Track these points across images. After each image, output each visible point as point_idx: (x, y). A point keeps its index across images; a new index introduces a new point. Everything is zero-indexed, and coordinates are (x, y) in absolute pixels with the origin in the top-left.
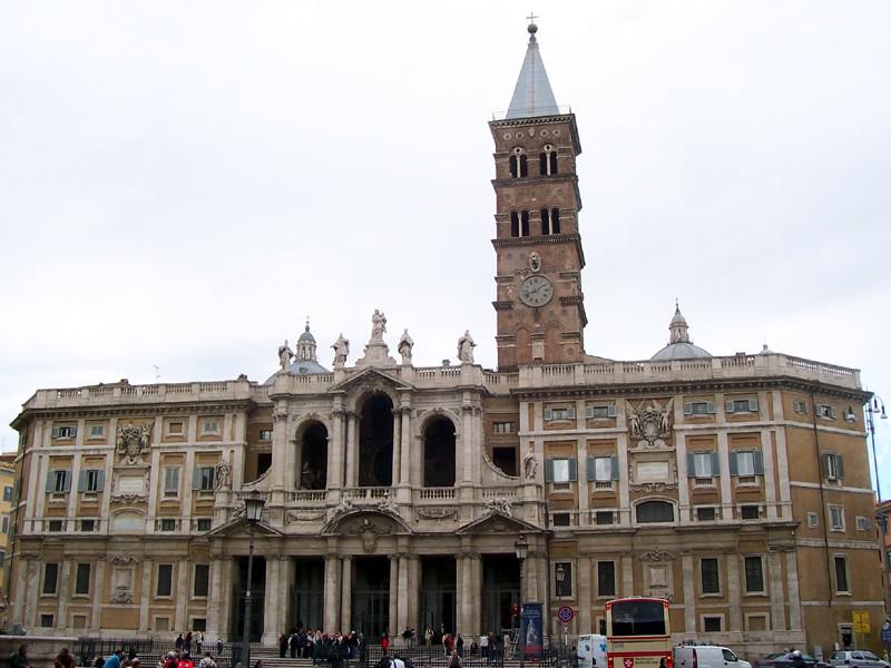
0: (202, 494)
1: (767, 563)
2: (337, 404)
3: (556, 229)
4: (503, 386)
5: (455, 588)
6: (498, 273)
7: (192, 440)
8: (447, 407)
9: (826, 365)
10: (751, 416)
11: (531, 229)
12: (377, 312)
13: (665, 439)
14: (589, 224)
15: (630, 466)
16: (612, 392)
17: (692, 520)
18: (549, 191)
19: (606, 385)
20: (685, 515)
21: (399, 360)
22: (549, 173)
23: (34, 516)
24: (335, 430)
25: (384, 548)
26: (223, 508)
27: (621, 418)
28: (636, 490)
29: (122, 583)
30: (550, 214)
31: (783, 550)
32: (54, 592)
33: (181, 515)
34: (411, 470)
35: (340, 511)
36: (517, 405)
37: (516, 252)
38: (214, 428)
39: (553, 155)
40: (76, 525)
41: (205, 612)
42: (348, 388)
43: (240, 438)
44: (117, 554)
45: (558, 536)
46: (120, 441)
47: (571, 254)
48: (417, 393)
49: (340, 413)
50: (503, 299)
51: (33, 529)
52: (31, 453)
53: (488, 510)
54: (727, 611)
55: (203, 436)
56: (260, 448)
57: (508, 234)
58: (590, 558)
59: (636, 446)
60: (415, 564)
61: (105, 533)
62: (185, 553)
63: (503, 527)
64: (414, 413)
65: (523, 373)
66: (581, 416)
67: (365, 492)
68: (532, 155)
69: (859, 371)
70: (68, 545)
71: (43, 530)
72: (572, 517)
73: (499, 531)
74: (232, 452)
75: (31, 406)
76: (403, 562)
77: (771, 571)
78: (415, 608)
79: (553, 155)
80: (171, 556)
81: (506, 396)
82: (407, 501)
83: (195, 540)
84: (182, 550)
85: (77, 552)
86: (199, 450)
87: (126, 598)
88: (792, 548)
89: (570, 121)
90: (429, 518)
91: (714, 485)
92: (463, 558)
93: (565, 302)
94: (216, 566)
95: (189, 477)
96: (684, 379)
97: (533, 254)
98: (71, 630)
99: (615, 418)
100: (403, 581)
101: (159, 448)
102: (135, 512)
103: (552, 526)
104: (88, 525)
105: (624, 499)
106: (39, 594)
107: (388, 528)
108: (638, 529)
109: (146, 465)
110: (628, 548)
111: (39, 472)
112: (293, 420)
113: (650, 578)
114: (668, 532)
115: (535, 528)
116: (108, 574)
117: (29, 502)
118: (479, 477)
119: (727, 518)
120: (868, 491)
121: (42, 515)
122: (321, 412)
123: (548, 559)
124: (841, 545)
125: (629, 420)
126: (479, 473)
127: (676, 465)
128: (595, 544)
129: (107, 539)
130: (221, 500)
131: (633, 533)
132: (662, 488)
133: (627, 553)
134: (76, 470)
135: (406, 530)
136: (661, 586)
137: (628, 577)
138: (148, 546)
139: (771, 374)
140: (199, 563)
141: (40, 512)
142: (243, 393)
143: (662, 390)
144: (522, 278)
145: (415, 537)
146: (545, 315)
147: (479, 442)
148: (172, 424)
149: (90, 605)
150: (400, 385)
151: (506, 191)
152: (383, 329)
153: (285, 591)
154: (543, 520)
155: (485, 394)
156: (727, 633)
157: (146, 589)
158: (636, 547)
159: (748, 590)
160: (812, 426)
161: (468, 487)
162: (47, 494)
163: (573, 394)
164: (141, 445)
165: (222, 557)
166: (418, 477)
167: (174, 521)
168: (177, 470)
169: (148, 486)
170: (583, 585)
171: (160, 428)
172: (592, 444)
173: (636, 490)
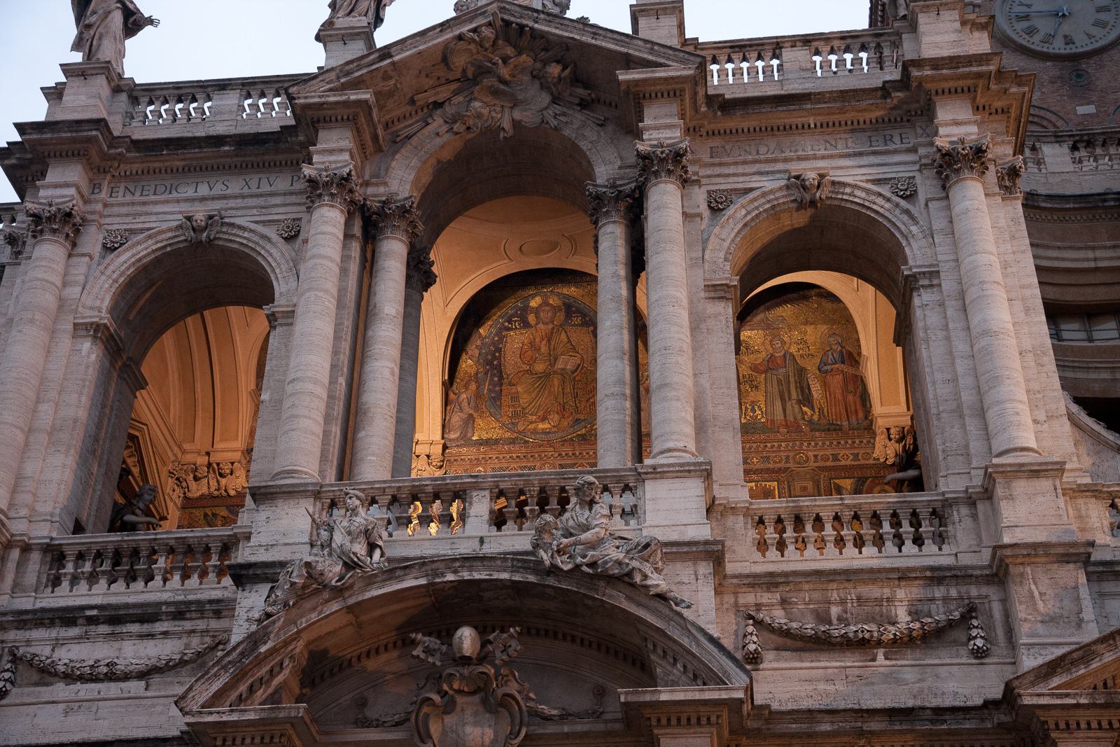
35: (314, 584)
107: (581, 701)
112: (109, 249)
135: (701, 675)
161: (1035, 473)
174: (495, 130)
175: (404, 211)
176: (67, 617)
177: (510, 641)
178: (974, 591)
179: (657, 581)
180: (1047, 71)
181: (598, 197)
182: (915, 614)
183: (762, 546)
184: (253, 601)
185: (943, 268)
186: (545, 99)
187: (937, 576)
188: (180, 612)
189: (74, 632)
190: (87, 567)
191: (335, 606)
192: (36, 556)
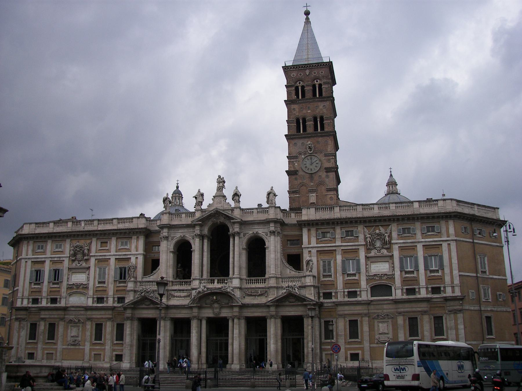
0: (120, 282)
1: (446, 319)
2: (197, 230)
3: (322, 128)
4: (293, 219)
5: (266, 336)
6: (289, 154)
7: (113, 252)
8: (261, 231)
9: (479, 205)
10: (436, 235)
11: (308, 128)
12: (219, 177)
14: (340, 124)
15: (366, 265)
16: (356, 222)
17: (403, 295)
18: (317, 107)
19: (353, 218)
20: (399, 292)
21: (233, 204)
22: (318, 96)
23: (23, 296)
24: (196, 245)
25: (225, 313)
26: (132, 290)
27: (361, 237)
28: (370, 278)
29: (74, 333)
30: (318, 120)
31: (456, 312)
32: (35, 339)
33: (108, 294)
34: (240, 268)
35: (199, 292)
36: (301, 230)
37: (299, 142)
38: (126, 244)
39: (320, 85)
40: (47, 301)
41: (122, 350)
42: (203, 221)
43: (141, 250)
44: (71, 317)
45: (325, 305)
46: (72, 252)
47: (331, 143)
48: (243, 224)
49: (199, 235)
50: (292, 169)
51: (22, 303)
52: (21, 259)
53: (285, 291)
55: (120, 249)
56: (154, 256)
57: (294, 131)
58: (344, 318)
60: (243, 322)
61: (64, 306)
62: (111, 316)
63: (293, 300)
64: (242, 235)
65: (304, 211)
66: (338, 236)
67: (214, 280)
68: (308, 86)
69: (498, 208)
70: (43, 313)
71: (28, 303)
72: (333, 294)
73: (291, 302)
74: (137, 258)
75: (20, 232)
76: (236, 321)
77: (448, 324)
78: (243, 347)
79: (320, 85)
80: (102, 318)
81: (294, 225)
82: (238, 286)
83: (116, 309)
84: (108, 314)
85: (48, 316)
86: (117, 257)
87: (77, 342)
88: (460, 311)
89: (329, 65)
90: (251, 295)
91: (415, 275)
92: (271, 318)
93: (328, 170)
94: (128, 324)
95: (112, 273)
96: (397, 214)
97: (309, 142)
98: (45, 361)
99: (358, 236)
100: (236, 332)
101: (94, 256)
102: (81, 293)
103: (322, 300)
104: (54, 301)
105: (363, 284)
106: (26, 340)
108: (372, 301)
109: (87, 266)
110: (366, 312)
111: (25, 270)
113: (379, 329)
114: (389, 302)
115: (312, 300)
116: (66, 329)
117: (20, 288)
118: (279, 271)
119: (423, 294)
120: (504, 278)
121: (27, 295)
122: (188, 234)
123: (320, 318)
124: (489, 309)
125: (366, 238)
126: (279, 269)
127: (393, 263)
128: (347, 310)
129: (65, 309)
130: (130, 286)
131: (368, 303)
132: (385, 278)
133: (366, 315)
134: (47, 268)
135: (238, 303)
136: (385, 333)
137: (366, 328)
138: (89, 313)
139: (448, 211)
140: (119, 322)
141: (26, 294)
142: (142, 224)
143: (385, 220)
144: (303, 157)
145: (243, 306)
146: (316, 178)
147: (279, 251)
148: (101, 242)
149: (56, 347)
150: (233, 219)
151: (293, 106)
152: (223, 187)
153: (168, 338)
154: (316, 296)
155: (282, 224)
157: (88, 338)
158: (370, 311)
159: (435, 335)
160: (471, 240)
162: (30, 283)
163: (333, 223)
164: (84, 255)
165: (132, 319)
166: (244, 272)
167: (103, 298)
168: (105, 269)
169: (88, 278)
170: (341, 333)
171: (95, 245)
172: (345, 252)
173: (370, 278)
174: (217, 223)
175: (206, 236)
176: (175, 290)
177: (219, 298)
178: (267, 290)
179: (233, 293)
180: (308, 176)
181: (230, 234)
182: (261, 292)
183: (246, 283)
184: (194, 292)
185: (269, 247)
186: (223, 218)
187: (263, 288)
188: (186, 290)
189: (176, 292)
191: (202, 294)
192: (170, 282)
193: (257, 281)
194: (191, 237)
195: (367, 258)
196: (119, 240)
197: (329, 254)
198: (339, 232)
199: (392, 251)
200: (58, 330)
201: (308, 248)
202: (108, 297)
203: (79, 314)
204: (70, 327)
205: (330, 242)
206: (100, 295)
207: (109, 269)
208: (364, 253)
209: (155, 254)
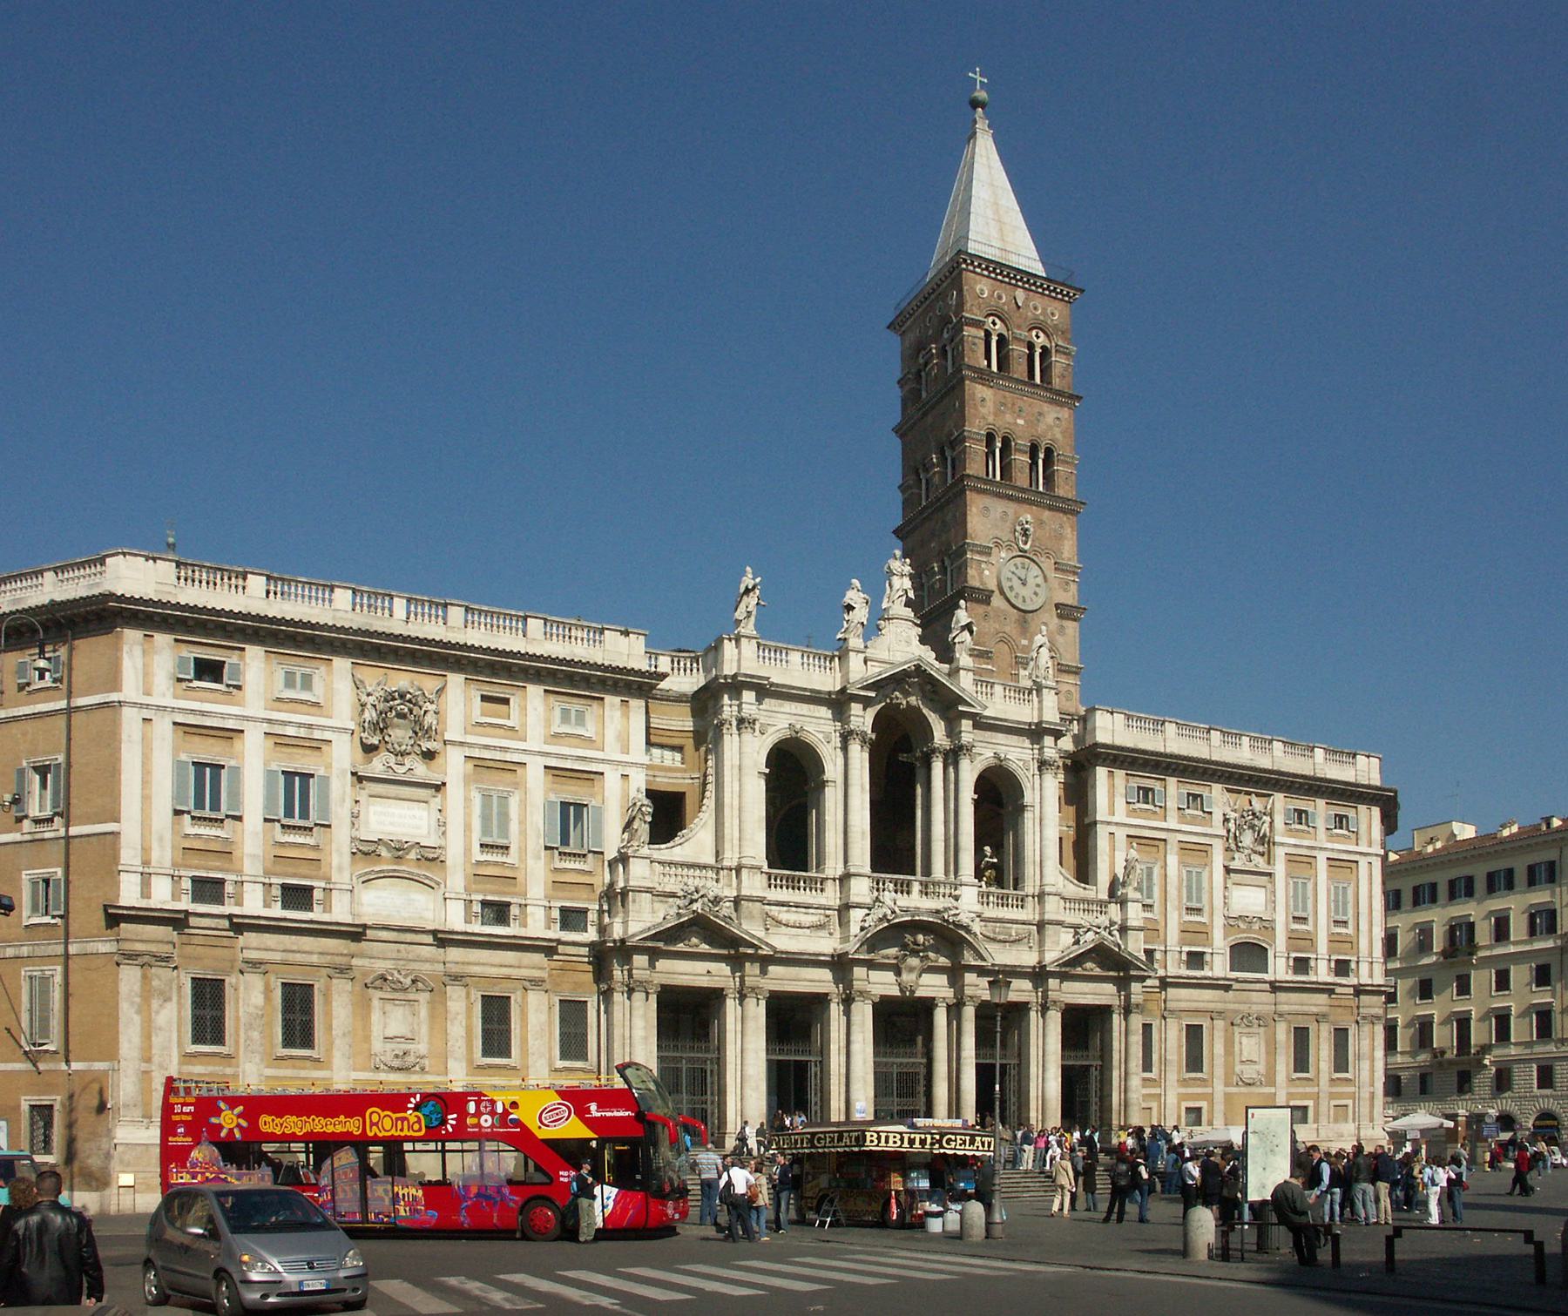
7: (535, 741)
8: (1018, 754)
13: (1262, 854)
17: (1287, 973)
20: (1281, 963)
26: (649, 890)
28: (1232, 923)
33: (525, 895)
44: (381, 966)
54: (1317, 1098)
55: (557, 735)
59: (1234, 859)
66: (1172, 804)
67: (908, 886)
74: (625, 776)
91: (1309, 927)
95: (537, 819)
99: (1210, 813)
108: (1236, 980)
110: (1219, 1006)
116: (362, 1008)
119: (1322, 972)
122: (818, 727)
125: (1226, 820)
127: (1274, 892)
129: (356, 934)
130: (639, 873)
132: (1256, 927)
138: (454, 953)
156: (1316, 1125)
168: (504, 800)
172: (1185, 848)
173: (1232, 923)
175: (871, 739)
181: (934, 751)
190: (778, 882)
193: (1002, 899)
194: (820, 736)
195: (1228, 870)
196: (552, 698)
197: (1148, 848)
198: (1174, 789)
199: (1272, 862)
200: (328, 1014)
201: (1109, 823)
202: (526, 905)
203: (410, 957)
204: (376, 1003)
205: (1152, 816)
206: (493, 893)
207: (523, 804)
208: (1221, 858)
209: (657, 773)
